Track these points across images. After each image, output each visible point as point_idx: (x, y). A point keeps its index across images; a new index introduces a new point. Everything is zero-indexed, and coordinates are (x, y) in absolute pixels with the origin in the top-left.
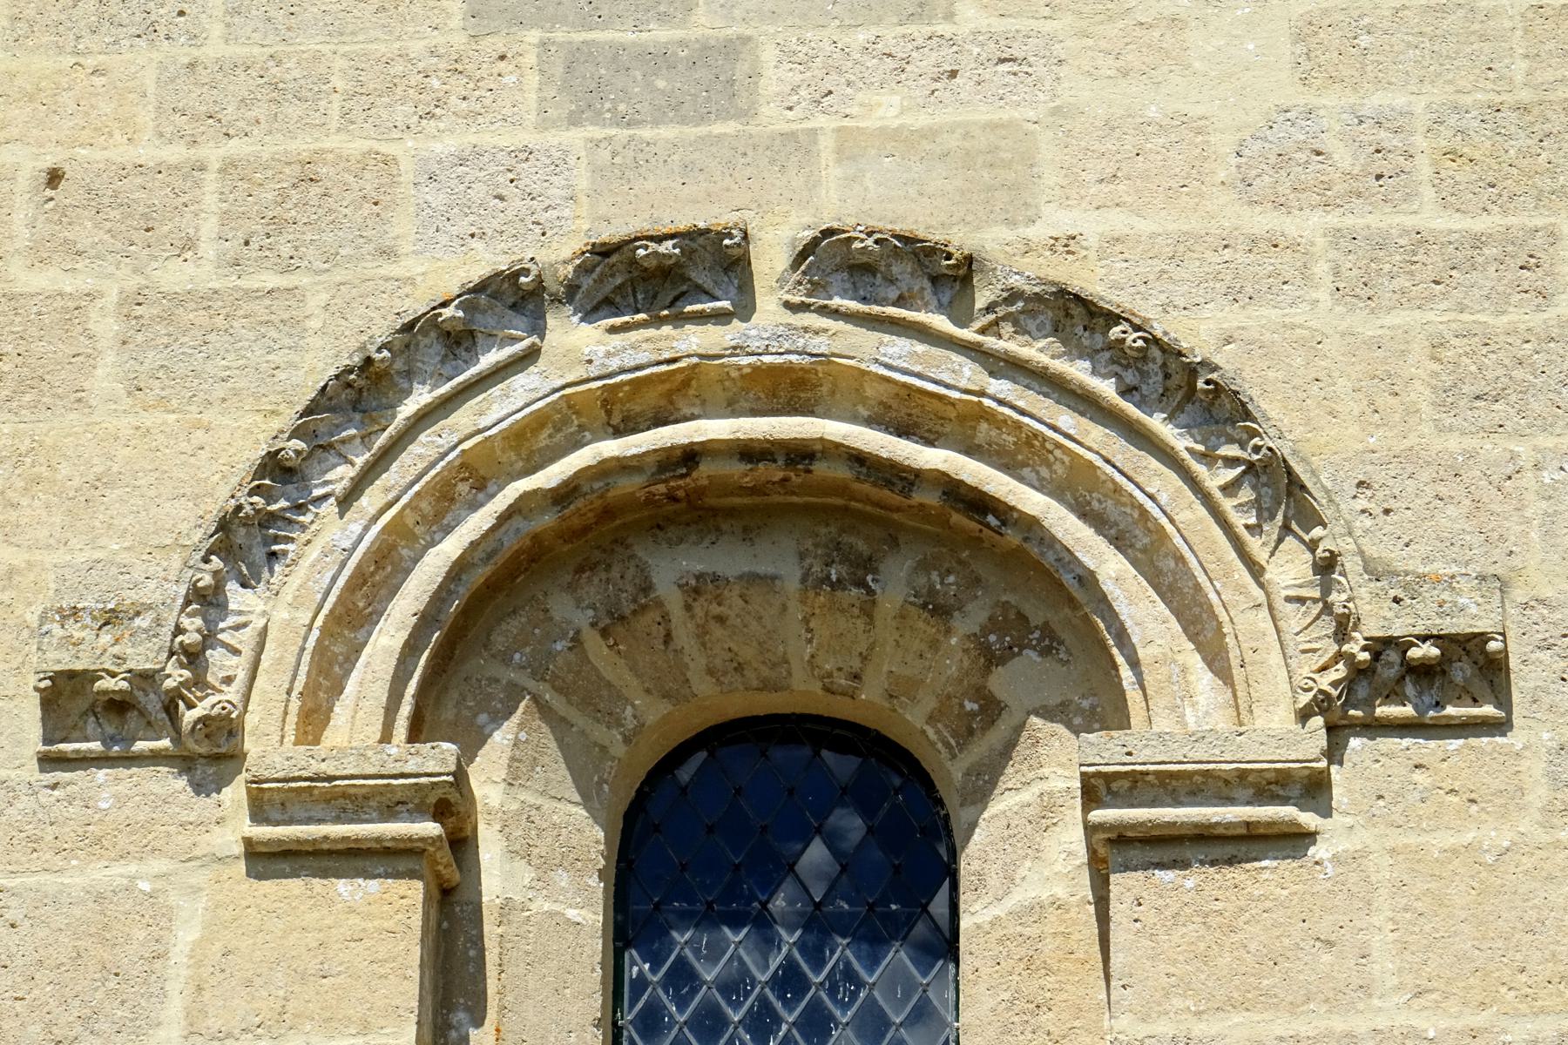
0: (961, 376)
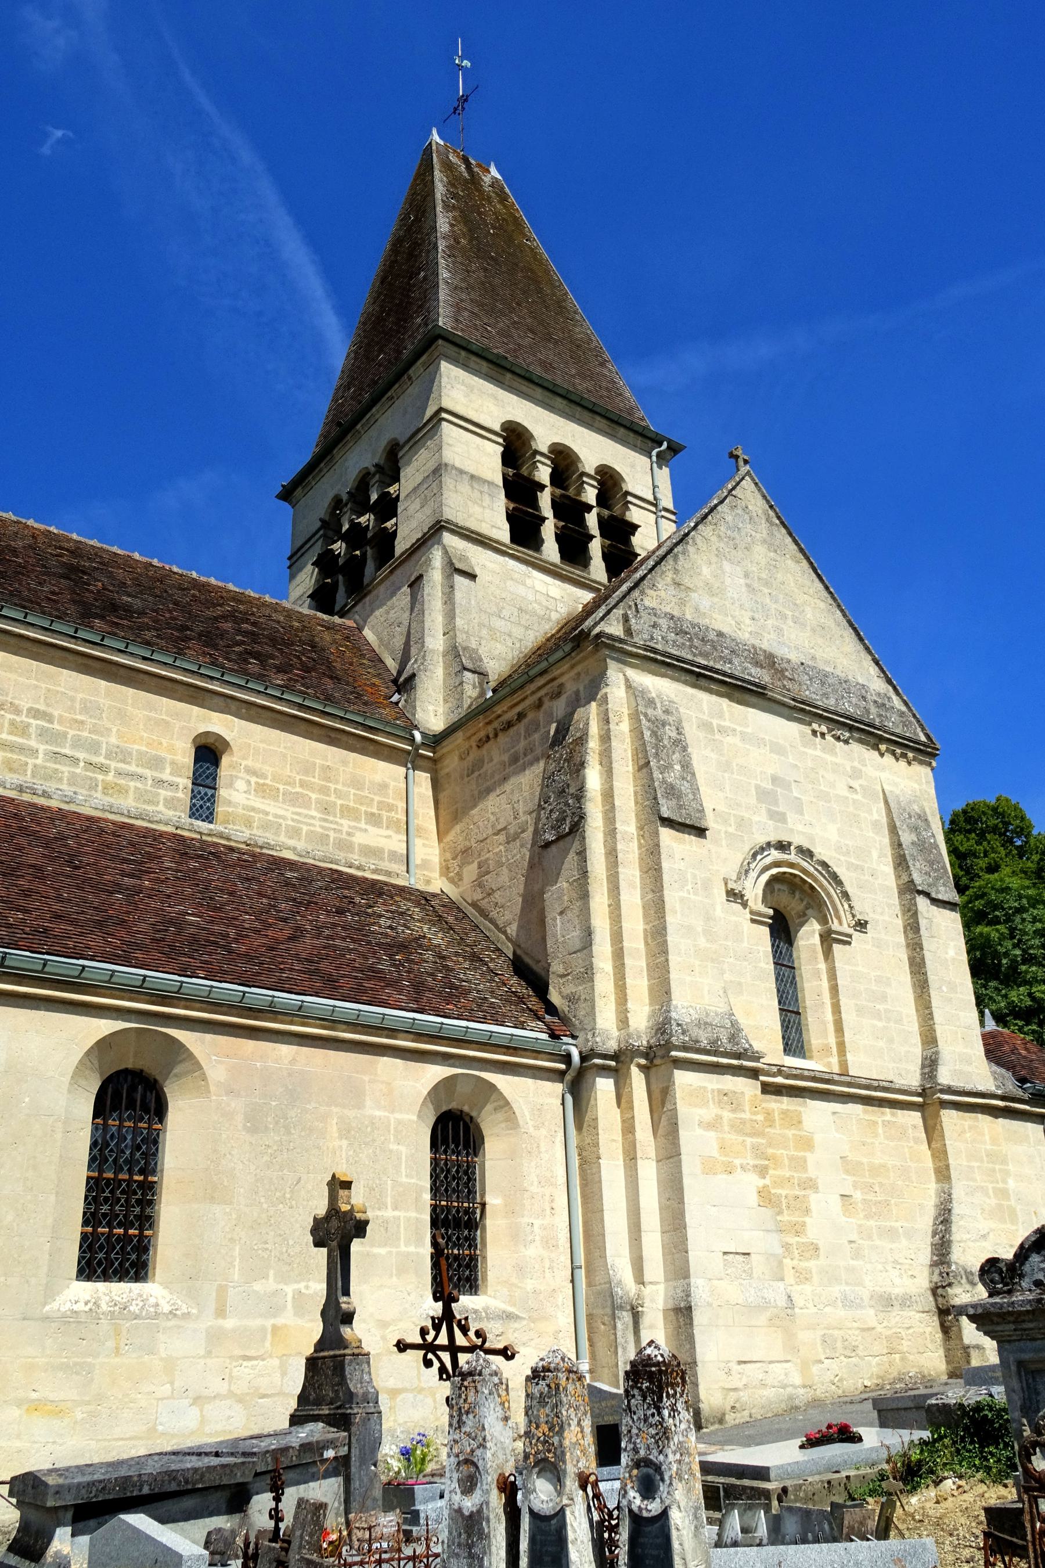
0: (811, 869)
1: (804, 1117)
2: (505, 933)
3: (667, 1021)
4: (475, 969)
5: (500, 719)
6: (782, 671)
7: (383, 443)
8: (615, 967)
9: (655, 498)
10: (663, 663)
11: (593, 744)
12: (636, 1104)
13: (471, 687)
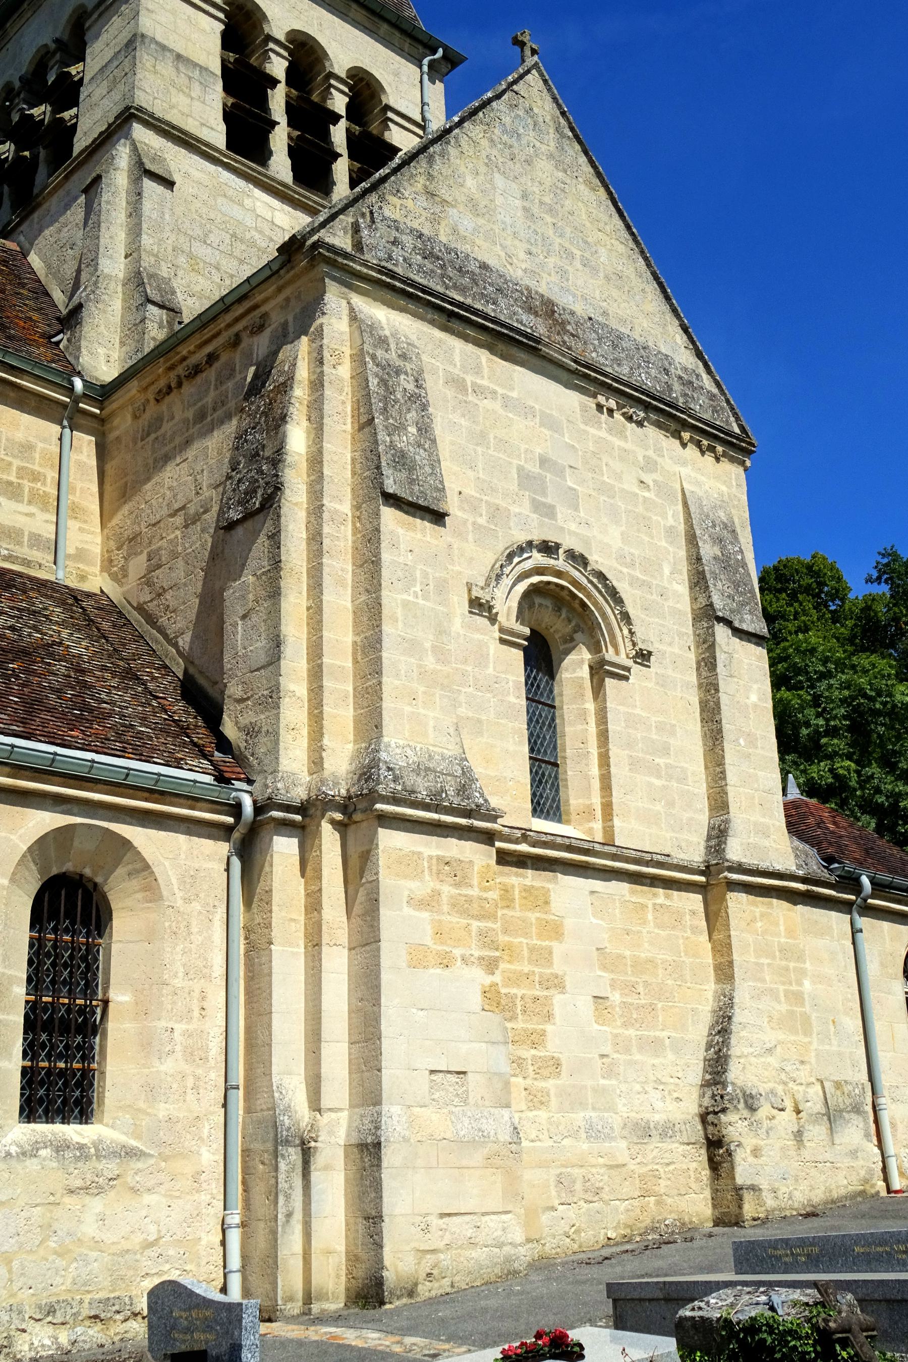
0: (584, 581)
1: (553, 897)
2: (175, 645)
3: (375, 763)
4: (126, 689)
5: (185, 363)
6: (563, 324)
7: (68, 11)
8: (311, 690)
9: (424, 119)
10: (403, 292)
11: (300, 392)
12: (325, 872)
13: (156, 326)
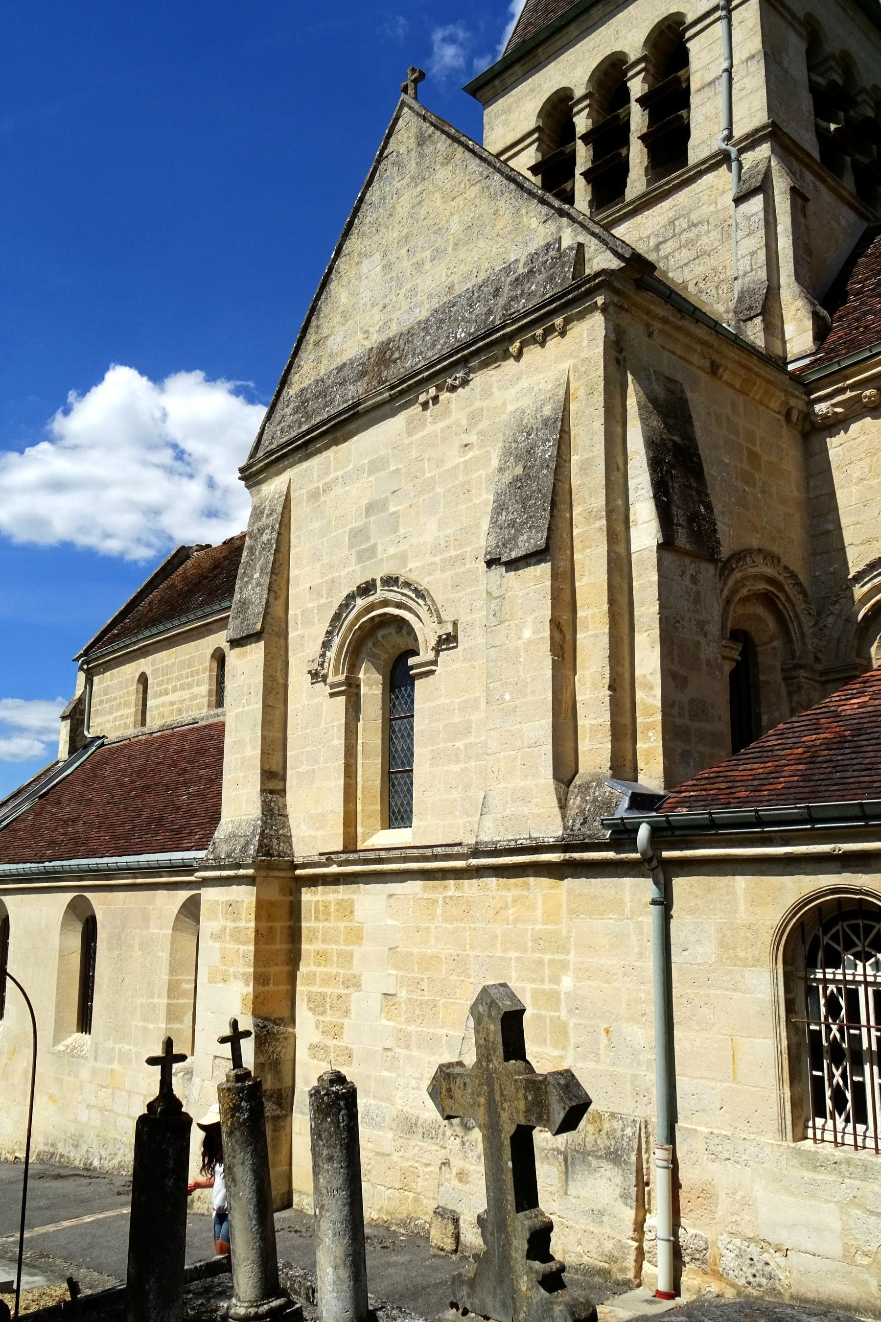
1: (357, 906)
